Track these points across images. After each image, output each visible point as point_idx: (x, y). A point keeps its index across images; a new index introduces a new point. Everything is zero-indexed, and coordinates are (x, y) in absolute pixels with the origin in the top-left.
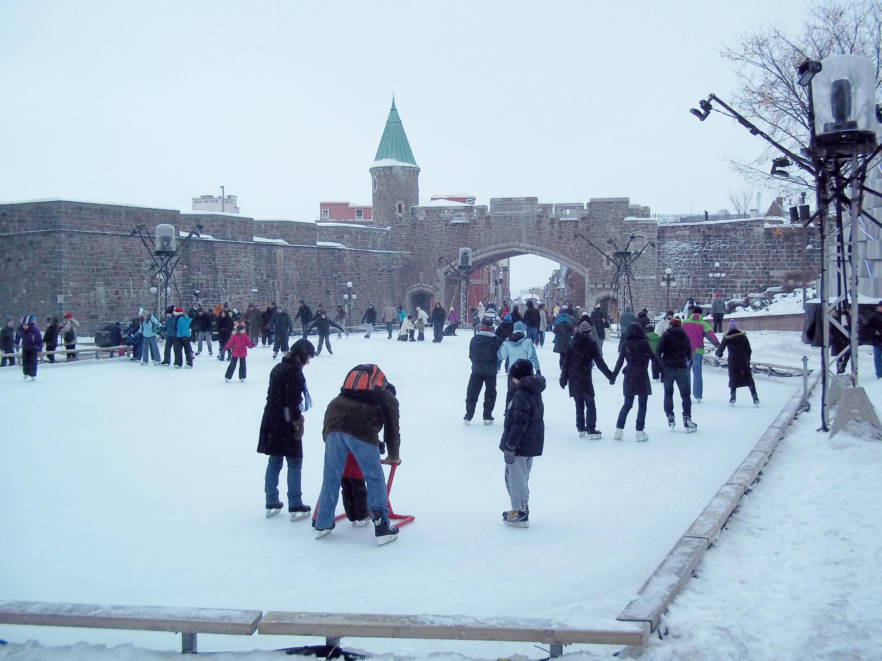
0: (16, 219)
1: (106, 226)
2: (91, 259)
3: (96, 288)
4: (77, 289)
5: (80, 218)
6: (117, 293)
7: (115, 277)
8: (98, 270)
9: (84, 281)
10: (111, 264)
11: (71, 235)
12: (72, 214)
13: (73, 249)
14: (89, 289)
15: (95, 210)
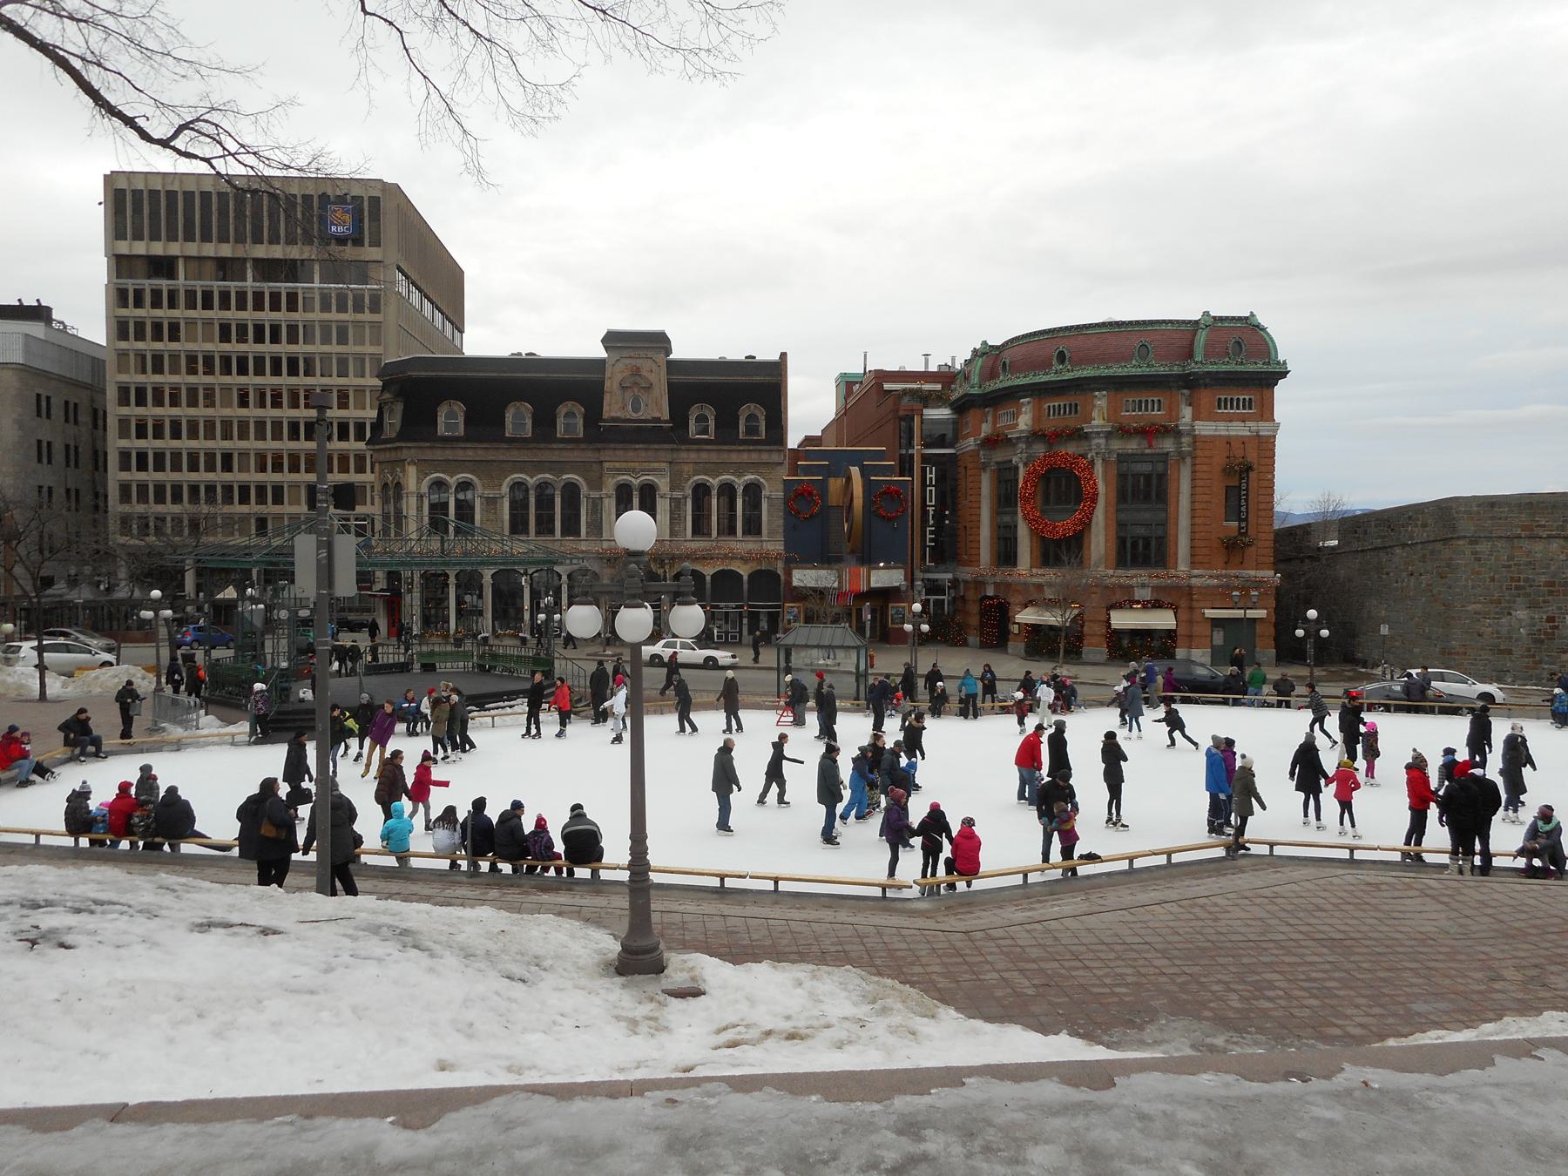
0: (1419, 523)
1: (1539, 526)
2: (1508, 572)
3: (1514, 613)
4: (1479, 614)
5: (1492, 518)
6: (1551, 619)
7: (1550, 598)
8: (1517, 588)
9: (1491, 602)
10: (1543, 579)
11: (1474, 540)
12: (1478, 513)
13: (1479, 559)
14: (1496, 613)
15: (1520, 505)
